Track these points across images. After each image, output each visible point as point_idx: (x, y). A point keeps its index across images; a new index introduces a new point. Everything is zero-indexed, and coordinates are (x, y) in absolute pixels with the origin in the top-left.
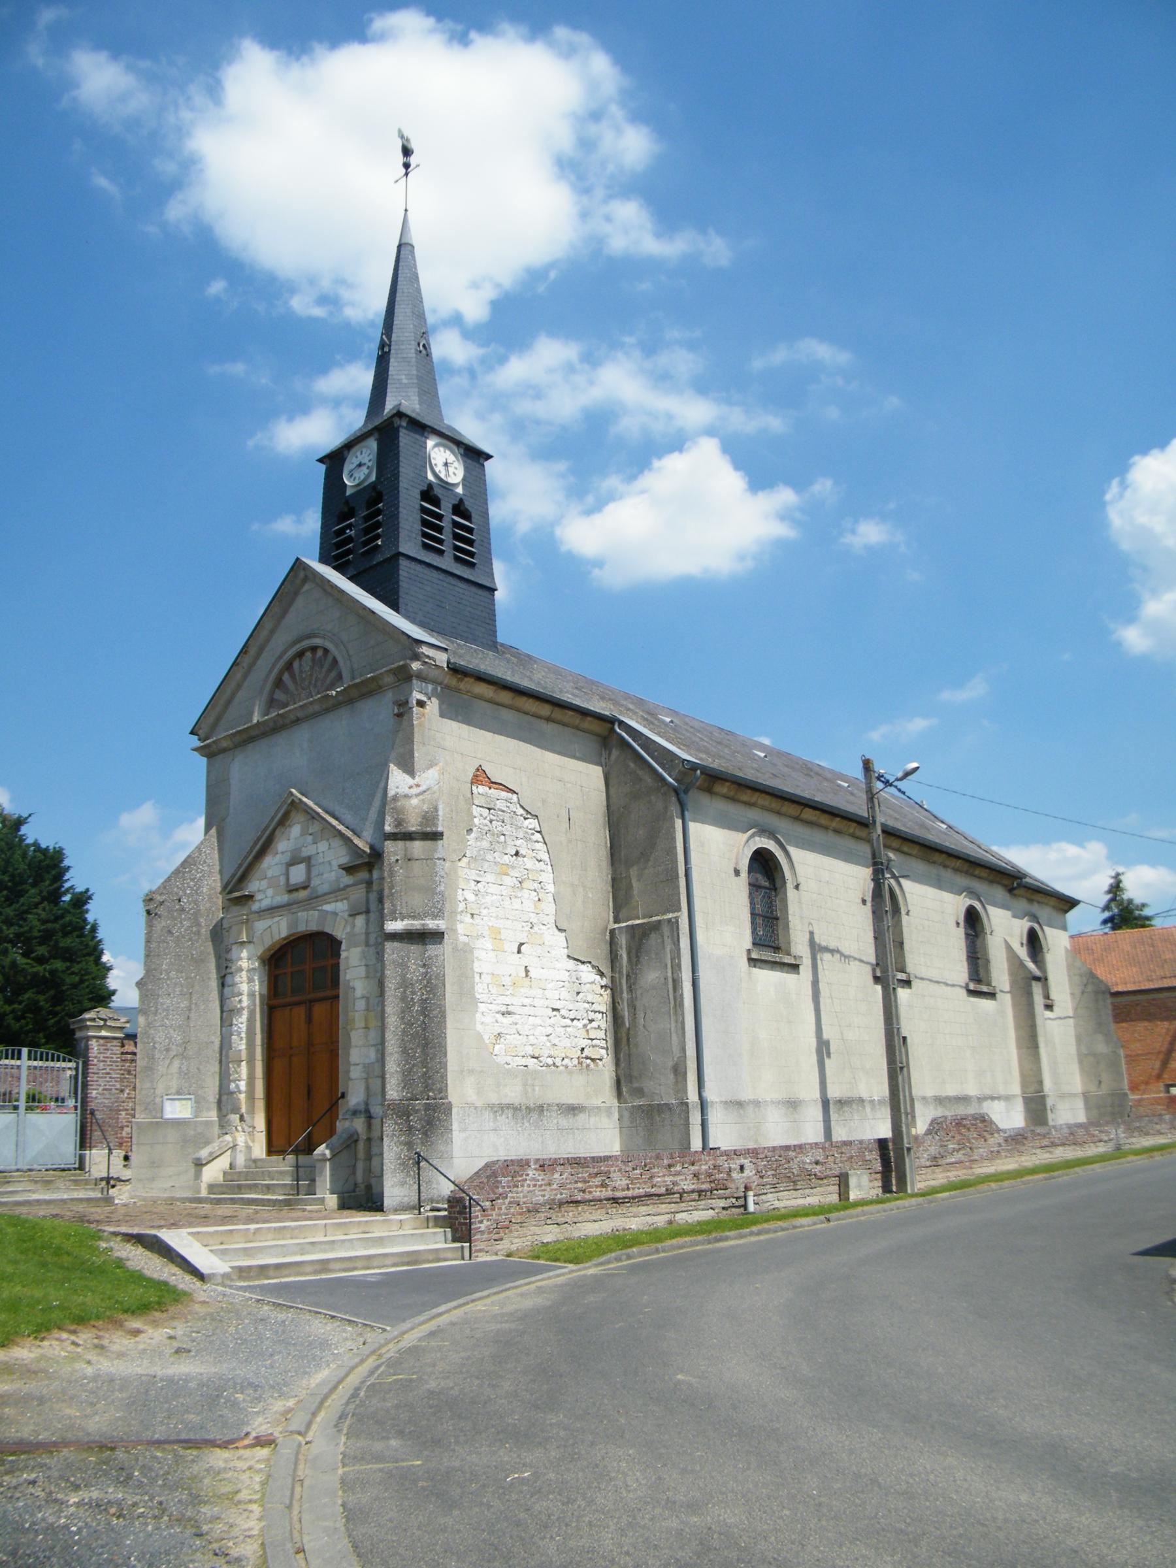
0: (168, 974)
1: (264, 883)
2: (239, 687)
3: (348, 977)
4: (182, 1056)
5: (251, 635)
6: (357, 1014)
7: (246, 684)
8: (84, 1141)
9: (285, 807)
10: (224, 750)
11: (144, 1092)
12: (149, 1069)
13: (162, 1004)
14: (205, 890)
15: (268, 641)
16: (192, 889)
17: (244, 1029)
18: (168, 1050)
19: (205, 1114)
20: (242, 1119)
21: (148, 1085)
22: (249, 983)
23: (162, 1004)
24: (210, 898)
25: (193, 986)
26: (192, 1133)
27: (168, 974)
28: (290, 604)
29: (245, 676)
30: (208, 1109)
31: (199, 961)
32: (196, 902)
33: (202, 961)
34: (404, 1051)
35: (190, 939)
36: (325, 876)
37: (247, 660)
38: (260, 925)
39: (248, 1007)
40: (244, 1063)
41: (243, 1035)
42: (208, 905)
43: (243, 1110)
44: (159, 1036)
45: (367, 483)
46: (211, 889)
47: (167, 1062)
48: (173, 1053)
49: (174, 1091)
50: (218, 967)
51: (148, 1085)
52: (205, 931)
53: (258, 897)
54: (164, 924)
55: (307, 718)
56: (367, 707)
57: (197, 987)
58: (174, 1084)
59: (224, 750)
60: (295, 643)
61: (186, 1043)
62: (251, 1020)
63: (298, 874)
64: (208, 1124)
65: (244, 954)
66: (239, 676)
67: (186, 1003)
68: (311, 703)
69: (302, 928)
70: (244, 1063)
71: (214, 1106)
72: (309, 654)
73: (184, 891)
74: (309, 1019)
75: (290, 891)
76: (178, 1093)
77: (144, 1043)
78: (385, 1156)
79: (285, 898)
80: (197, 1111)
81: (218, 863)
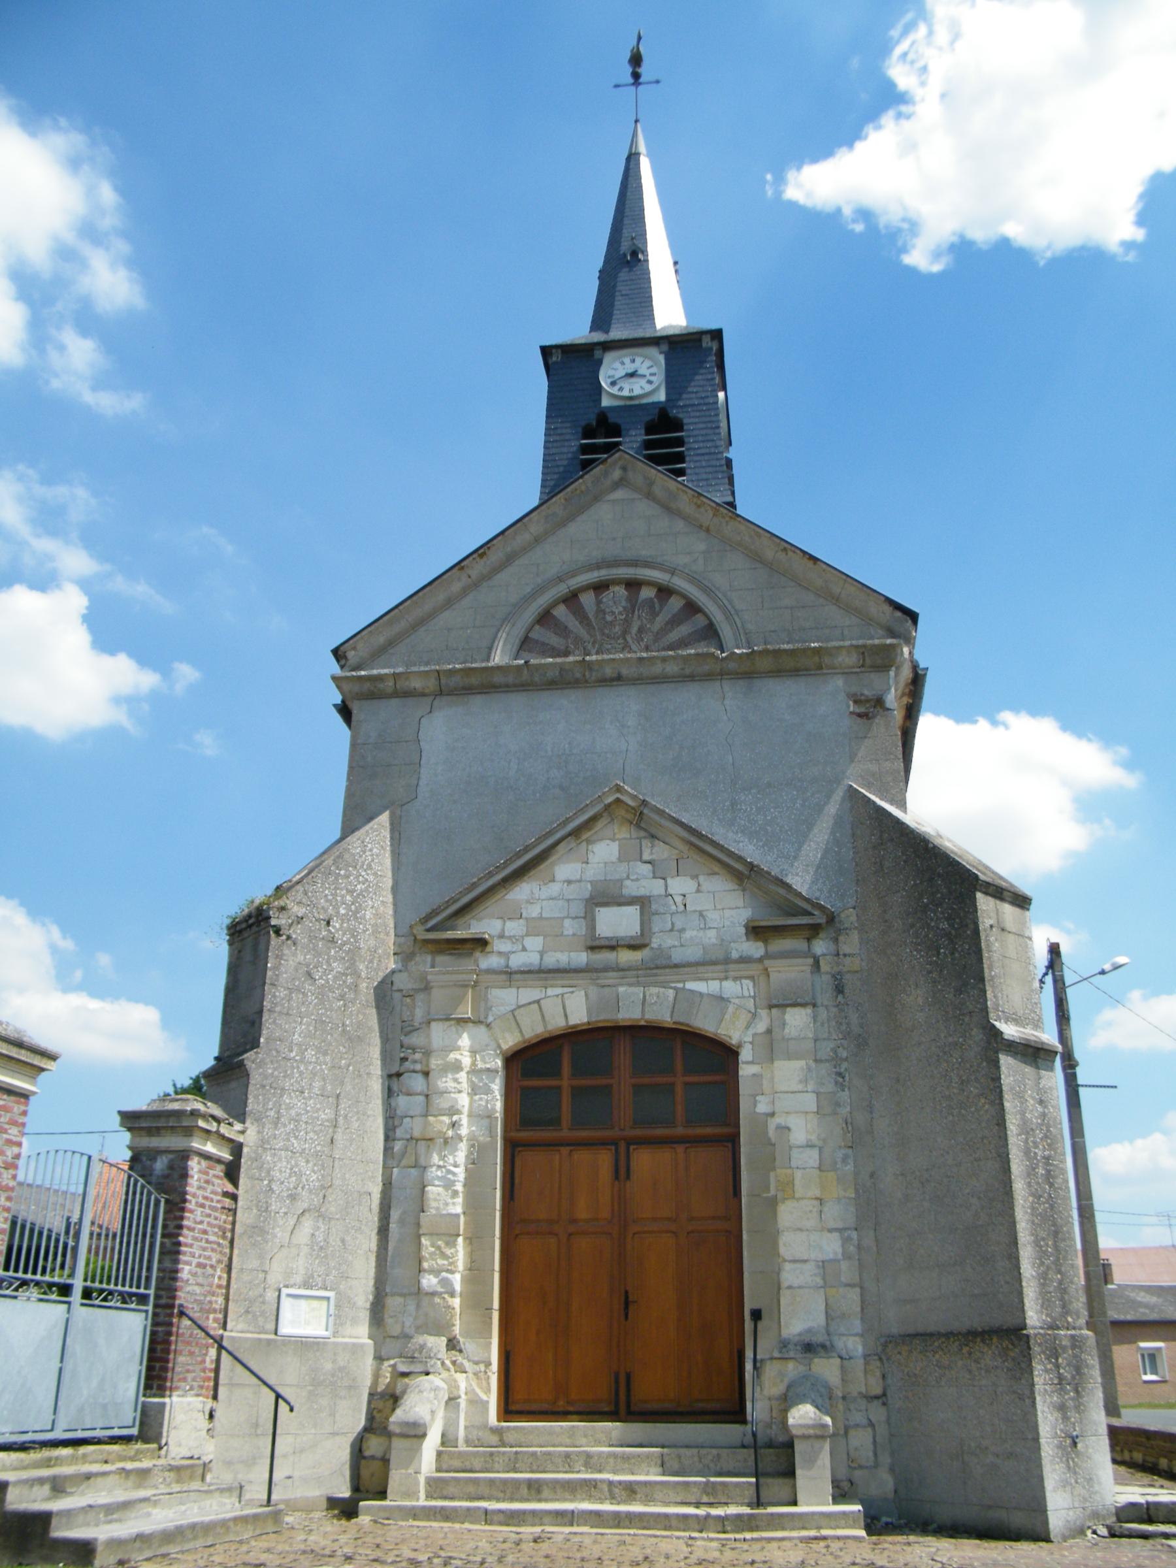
0: (302, 1053)
1: (514, 927)
2: (449, 603)
3: (762, 1107)
4: (319, 1213)
5: (502, 533)
6: (798, 1174)
7: (467, 601)
8: (157, 1372)
9: (598, 808)
10: (408, 694)
11: (246, 1277)
12: (259, 1230)
13: (289, 1107)
14: (368, 915)
15: (525, 549)
16: (348, 908)
17: (461, 1173)
18: (293, 1197)
19: (348, 1329)
20: (452, 1344)
21: (254, 1263)
22: (469, 1089)
23: (289, 1107)
24: (375, 932)
25: (342, 1083)
26: (328, 1366)
27: (302, 1053)
28: (582, 509)
29: (465, 591)
30: (355, 1321)
31: (354, 1040)
32: (353, 932)
33: (360, 1039)
34: (1037, 1243)
35: (342, 997)
36: (688, 934)
37: (478, 568)
38: (504, 998)
39: (472, 1138)
40: (460, 1240)
41: (459, 1187)
42: (372, 943)
43: (457, 1330)
44: (281, 1169)
45: (644, 401)
46: (377, 915)
47: (292, 1222)
48: (301, 1205)
49: (298, 1279)
50: (385, 1056)
51: (254, 1263)
52: (366, 989)
53: (498, 946)
54: (300, 958)
55: (637, 681)
56: (782, 696)
57: (348, 1087)
58: (301, 1266)
59: (408, 694)
60: (598, 566)
61: (325, 1187)
62: (475, 1164)
63: (618, 922)
64: (355, 1349)
65: (465, 1041)
66: (456, 587)
67: (327, 1114)
68: (664, 660)
69: (629, 1013)
70: (460, 1240)
71: (365, 1316)
72: (620, 591)
73: (336, 908)
74: (26, 1175)
75: (592, 948)
76: (307, 1285)
77: (252, 1178)
78: (1041, 1429)
79: (582, 958)
80: (338, 1319)
81: (390, 874)
